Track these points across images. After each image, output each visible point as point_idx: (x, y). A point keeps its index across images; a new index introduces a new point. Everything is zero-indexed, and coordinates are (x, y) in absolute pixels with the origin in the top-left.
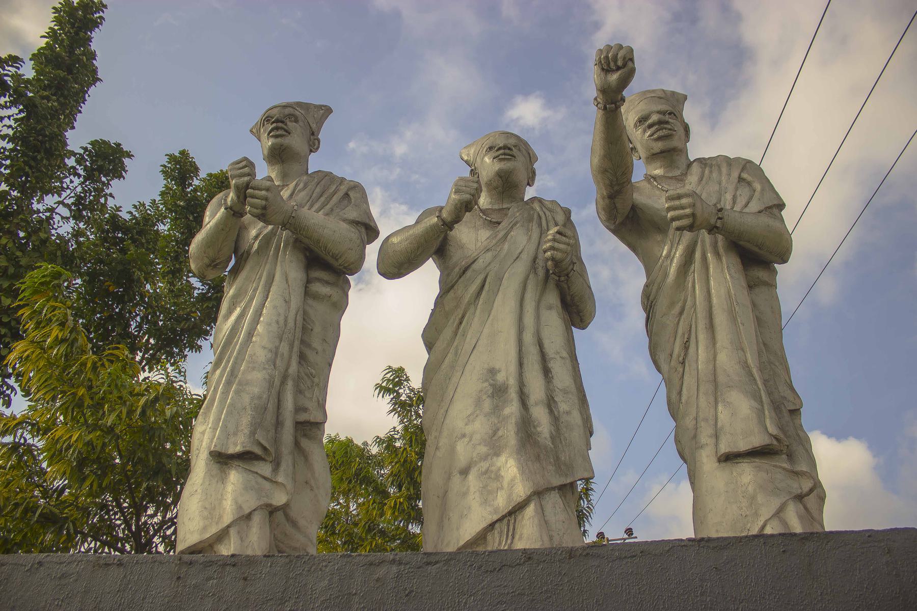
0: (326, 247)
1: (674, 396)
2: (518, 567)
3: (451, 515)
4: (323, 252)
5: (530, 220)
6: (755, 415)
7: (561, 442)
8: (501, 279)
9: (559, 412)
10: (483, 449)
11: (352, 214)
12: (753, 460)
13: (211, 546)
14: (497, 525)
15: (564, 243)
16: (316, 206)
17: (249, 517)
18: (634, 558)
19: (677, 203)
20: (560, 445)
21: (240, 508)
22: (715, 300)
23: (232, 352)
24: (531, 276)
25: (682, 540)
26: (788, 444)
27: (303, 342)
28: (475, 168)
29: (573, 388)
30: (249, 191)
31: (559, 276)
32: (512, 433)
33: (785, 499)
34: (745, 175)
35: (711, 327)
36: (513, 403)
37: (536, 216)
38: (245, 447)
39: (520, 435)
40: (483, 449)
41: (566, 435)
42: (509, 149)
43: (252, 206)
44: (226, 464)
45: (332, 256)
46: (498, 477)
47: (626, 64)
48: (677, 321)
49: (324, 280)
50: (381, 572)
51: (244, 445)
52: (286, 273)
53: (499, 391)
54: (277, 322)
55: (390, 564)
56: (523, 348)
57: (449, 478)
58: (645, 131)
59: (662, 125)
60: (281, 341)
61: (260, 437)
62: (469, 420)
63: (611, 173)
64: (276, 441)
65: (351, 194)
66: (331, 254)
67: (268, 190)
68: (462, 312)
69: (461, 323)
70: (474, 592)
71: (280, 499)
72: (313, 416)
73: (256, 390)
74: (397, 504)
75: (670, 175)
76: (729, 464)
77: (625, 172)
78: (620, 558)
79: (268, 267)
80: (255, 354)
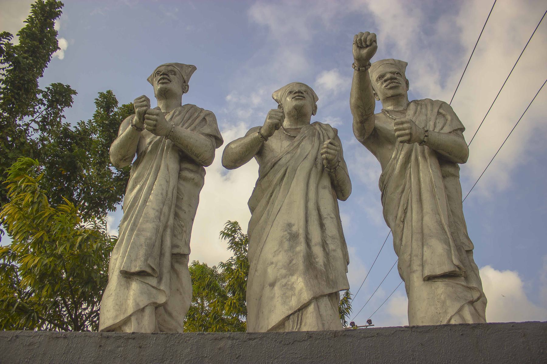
0: (192, 150)
1: (398, 241)
2: (303, 342)
3: (264, 310)
4: (190, 152)
5: (314, 135)
6: (446, 253)
7: (330, 268)
8: (296, 171)
9: (329, 250)
10: (283, 271)
11: (207, 130)
12: (444, 280)
13: (120, 327)
14: (291, 317)
15: (334, 150)
16: (186, 125)
17: (143, 310)
18: (373, 338)
19: (401, 126)
20: (329, 270)
21: (137, 304)
22: (423, 185)
23: (134, 212)
24: (314, 169)
25: (401, 327)
26: (465, 271)
27: (177, 206)
28: (281, 104)
29: (337, 236)
30: (146, 115)
31: (330, 169)
32: (301, 262)
33: (463, 303)
34: (441, 111)
35: (420, 201)
36: (302, 244)
37: (317, 133)
38: (142, 268)
39: (306, 263)
40: (283, 271)
41: (333, 264)
42: (302, 93)
43: (148, 124)
44: (130, 278)
45: (195, 155)
46: (292, 288)
47: (372, 43)
48: (400, 197)
49: (190, 169)
50: (222, 344)
51: (141, 267)
52: (167, 165)
53: (293, 237)
54: (162, 194)
55: (227, 339)
56: (308, 211)
57: (263, 288)
58: (382, 84)
59: (393, 80)
60: (164, 205)
61: (150, 262)
62: (276, 253)
63: (362, 108)
64: (160, 265)
65: (207, 118)
66: (194, 154)
67: (157, 115)
68: (272, 189)
69: (271, 196)
70: (277, 356)
71: (162, 299)
72: (182, 250)
73: (148, 234)
74: (232, 303)
75: (397, 110)
76: (430, 282)
77: (370, 108)
78: (365, 338)
79: (157, 160)
80: (148, 213)
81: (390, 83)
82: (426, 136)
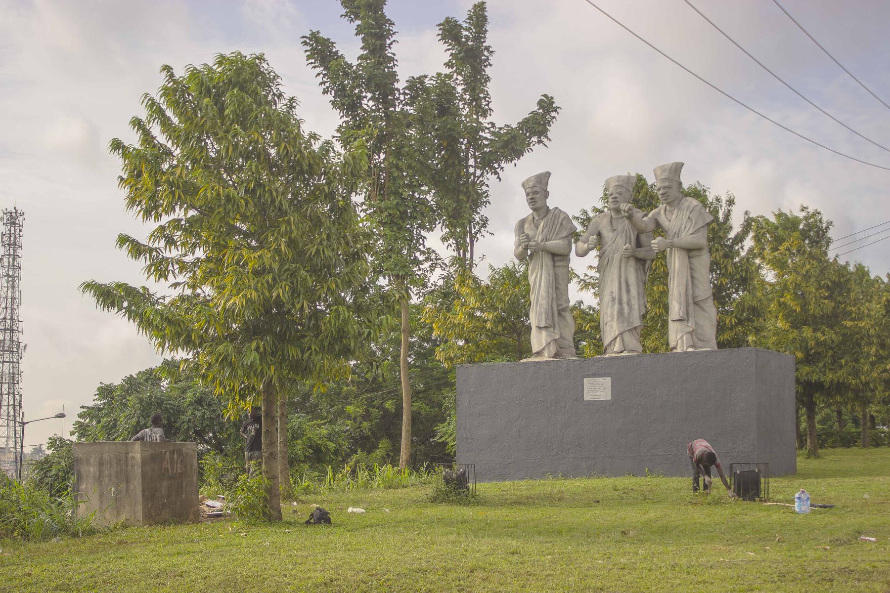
10: (609, 319)
17: (549, 343)
21: (547, 341)
35: (674, 277)
53: (613, 299)
61: (548, 322)
64: (553, 320)
65: (564, 223)
71: (557, 337)
72: (565, 305)
73: (545, 306)
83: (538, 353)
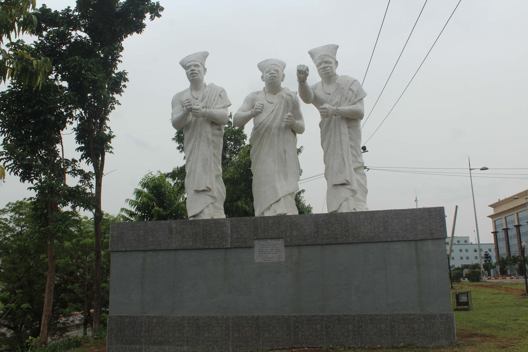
14: (273, 205)
30: (192, 110)
44: (198, 192)
81: (323, 71)
82: (337, 112)
83: (194, 216)
